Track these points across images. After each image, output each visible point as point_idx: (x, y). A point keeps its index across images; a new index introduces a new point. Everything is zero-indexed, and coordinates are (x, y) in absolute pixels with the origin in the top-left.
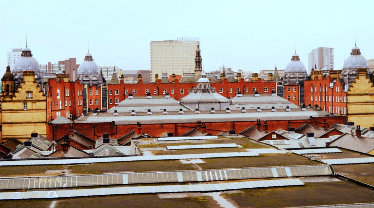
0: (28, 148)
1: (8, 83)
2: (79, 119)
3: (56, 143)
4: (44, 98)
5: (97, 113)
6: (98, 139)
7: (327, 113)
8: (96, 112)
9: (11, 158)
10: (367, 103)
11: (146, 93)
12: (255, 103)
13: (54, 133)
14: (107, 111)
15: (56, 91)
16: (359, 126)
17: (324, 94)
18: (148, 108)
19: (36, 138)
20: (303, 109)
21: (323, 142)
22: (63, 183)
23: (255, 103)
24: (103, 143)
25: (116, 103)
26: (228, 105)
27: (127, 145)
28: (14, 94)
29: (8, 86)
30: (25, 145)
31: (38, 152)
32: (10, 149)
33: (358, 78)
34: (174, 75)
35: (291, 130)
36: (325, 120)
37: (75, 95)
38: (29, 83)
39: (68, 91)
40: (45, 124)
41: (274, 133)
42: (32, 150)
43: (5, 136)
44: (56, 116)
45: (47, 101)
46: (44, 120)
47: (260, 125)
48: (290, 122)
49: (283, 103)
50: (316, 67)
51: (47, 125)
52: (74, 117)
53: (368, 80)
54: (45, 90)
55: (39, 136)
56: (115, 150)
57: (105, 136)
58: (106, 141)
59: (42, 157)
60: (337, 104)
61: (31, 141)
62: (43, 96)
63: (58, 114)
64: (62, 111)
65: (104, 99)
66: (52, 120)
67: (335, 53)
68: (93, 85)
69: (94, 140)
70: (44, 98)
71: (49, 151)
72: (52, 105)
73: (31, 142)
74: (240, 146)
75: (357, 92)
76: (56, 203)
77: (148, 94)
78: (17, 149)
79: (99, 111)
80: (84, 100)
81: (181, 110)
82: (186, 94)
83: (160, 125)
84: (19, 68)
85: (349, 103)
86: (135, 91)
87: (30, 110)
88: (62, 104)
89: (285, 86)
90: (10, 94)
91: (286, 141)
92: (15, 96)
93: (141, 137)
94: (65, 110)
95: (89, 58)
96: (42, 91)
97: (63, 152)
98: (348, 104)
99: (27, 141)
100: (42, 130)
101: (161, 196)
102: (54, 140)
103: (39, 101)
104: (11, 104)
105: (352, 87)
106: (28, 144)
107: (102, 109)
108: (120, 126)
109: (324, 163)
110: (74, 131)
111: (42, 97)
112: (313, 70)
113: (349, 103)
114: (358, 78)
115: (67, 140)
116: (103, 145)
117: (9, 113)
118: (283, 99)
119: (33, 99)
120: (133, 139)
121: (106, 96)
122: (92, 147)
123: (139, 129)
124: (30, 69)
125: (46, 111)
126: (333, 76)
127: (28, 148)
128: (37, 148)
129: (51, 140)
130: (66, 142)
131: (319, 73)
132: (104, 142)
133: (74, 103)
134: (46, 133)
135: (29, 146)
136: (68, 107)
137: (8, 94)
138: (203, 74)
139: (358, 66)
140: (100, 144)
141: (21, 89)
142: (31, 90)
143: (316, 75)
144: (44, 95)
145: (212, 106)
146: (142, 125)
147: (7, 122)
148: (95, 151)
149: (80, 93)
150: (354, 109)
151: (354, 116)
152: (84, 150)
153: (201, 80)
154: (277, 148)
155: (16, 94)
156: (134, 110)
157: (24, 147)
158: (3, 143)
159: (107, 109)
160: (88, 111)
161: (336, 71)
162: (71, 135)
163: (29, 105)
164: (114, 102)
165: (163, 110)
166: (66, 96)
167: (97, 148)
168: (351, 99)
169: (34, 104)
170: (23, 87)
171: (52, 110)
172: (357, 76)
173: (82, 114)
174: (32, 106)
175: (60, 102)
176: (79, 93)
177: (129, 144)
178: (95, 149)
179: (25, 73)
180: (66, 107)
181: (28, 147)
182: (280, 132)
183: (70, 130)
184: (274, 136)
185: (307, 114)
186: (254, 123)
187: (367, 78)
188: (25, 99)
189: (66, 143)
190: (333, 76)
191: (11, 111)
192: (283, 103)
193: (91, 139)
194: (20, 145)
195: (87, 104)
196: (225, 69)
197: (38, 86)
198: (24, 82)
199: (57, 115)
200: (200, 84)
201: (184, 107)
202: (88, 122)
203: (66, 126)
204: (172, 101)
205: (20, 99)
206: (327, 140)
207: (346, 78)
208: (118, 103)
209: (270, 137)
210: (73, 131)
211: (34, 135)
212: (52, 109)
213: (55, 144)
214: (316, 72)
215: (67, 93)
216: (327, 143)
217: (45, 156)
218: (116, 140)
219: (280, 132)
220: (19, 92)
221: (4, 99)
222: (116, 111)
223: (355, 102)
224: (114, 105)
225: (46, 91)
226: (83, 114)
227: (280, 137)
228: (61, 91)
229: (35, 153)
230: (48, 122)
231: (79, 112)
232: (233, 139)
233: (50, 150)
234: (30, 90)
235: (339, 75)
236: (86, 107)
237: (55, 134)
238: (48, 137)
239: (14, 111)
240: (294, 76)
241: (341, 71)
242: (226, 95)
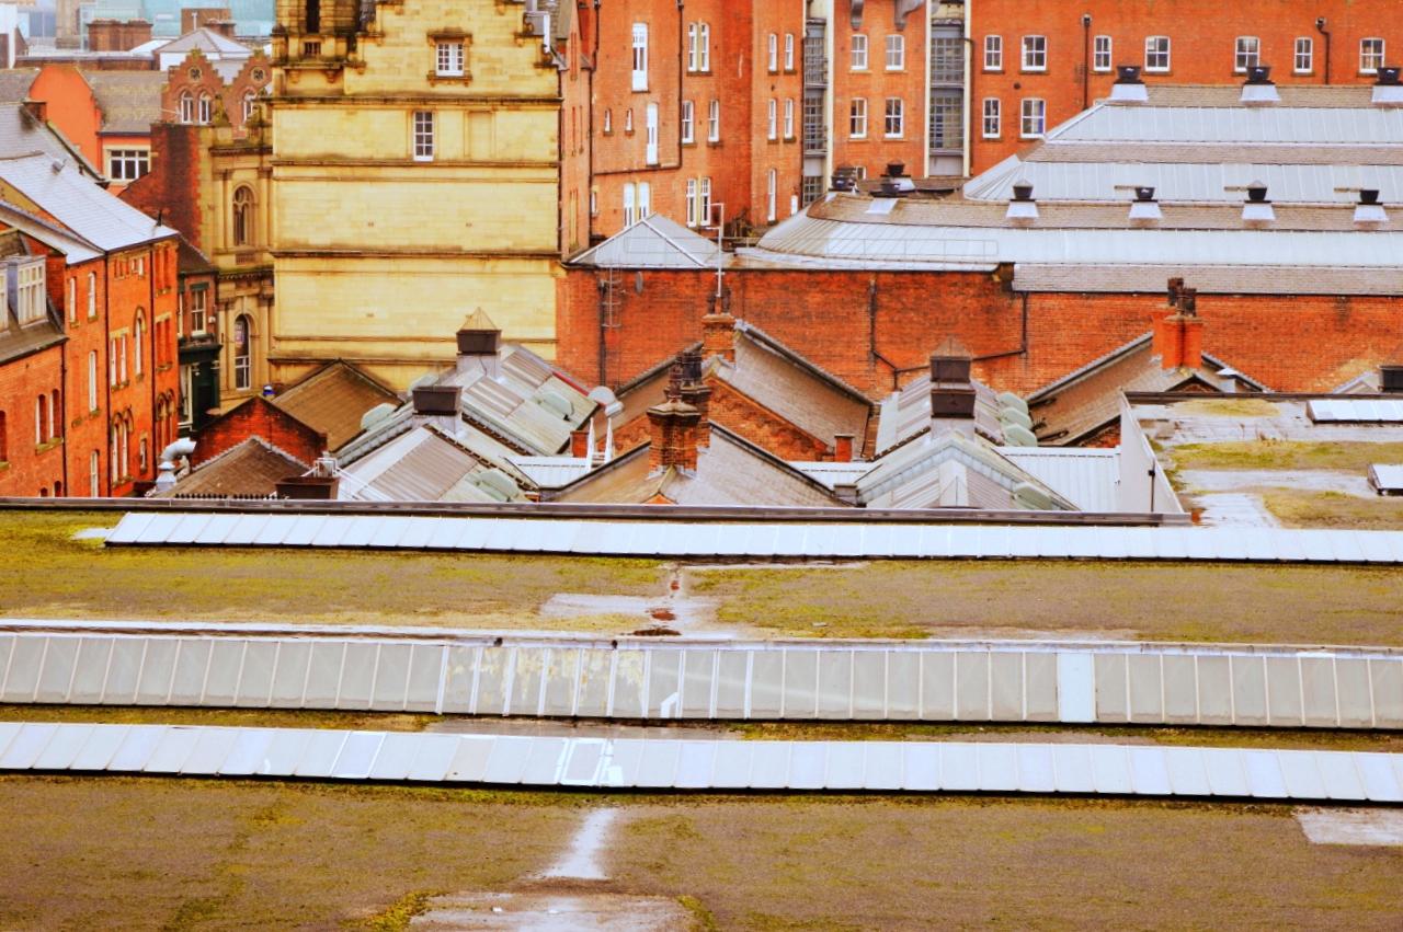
0: (434, 431)
2: (771, 237)
3: (618, 405)
4: (545, 83)
5: (893, 202)
6: (896, 388)
8: (889, 192)
9: (328, 497)
11: (1241, 60)
13: (603, 330)
14: (960, 189)
15: (625, 36)
18: (1251, 176)
19: (487, 360)
22: (661, 689)
24: (928, 421)
25: (1027, 130)
27: (1090, 438)
28: (352, 48)
30: (416, 406)
31: (500, 462)
32: (320, 430)
37: (749, 62)
39: (706, 33)
40: (546, 265)
42: (459, 446)
43: (289, 339)
44: (619, 214)
45: (565, 105)
51: (562, 273)
54: (554, 29)
55: (505, 351)
56: (1014, 472)
57: (941, 370)
58: (954, 406)
59: (522, 499)
61: (456, 381)
62: (537, 65)
63: (637, 195)
64: (658, 176)
65: (947, 98)
66: (595, 240)
69: (866, 396)
70: (545, 83)
71: (568, 458)
72: (598, 132)
73: (452, 394)
76: (615, 827)
77: (1252, 69)
78: (365, 431)
79: (905, 184)
80: (811, 106)
83: (1328, 307)
86: (1163, 46)
87: (453, 164)
88: (662, 124)
90: (330, 47)
92: (359, 66)
93: (1191, 389)
94: (680, 174)
96: (528, 33)
97: (661, 468)
99: (427, 384)
101: (1321, 828)
102: (602, 382)
103: (514, 102)
104: (332, 116)
106: (436, 402)
107: (926, 175)
108: (1050, 303)
110: (740, 325)
111: (531, 72)
115: (693, 386)
116: (927, 430)
117: (323, 184)
119: (477, 88)
120: (1136, 398)
121: (960, 77)
122: (856, 446)
123: (1183, 329)
125: (554, 173)
127: (434, 431)
128: (496, 436)
129: (584, 378)
130: (686, 398)
132: (937, 415)
133: (742, 121)
134: (551, 333)
135: (444, 419)
136: (702, 150)
137: (311, 50)
140: (904, 427)
141: (400, 13)
142: (465, 26)
144: (545, 64)
146: (1199, 303)
147: (308, 246)
148: (874, 477)
149: (781, 55)
152: (799, 465)
155: (366, 50)
156: (1152, 190)
157: (408, 424)
158: (278, 389)
159: (966, 174)
160: (837, 188)
162: (719, 352)
164: (1012, 123)
165: (1357, 197)
166: (693, 69)
167: (886, 453)
169: (481, 126)
171: (598, 168)
173: (795, 200)
174: (469, 137)
175: (652, 113)
177: (1105, 434)
178: (878, 457)
180: (684, 151)
181: (433, 421)
183: (710, 317)
188: (423, 86)
189: (682, 406)
193: (848, 386)
194: (386, 407)
195: (830, 135)
199: (629, 204)
202: (833, 265)
203: (686, 289)
205: (389, 83)
208: (1040, 131)
210: (727, 326)
211: (478, 343)
213: (608, 410)
215: (700, 57)
217: (542, 489)
218: (1017, 405)
220: (383, 35)
221: (291, 87)
222: (1023, 194)
224: (1019, 146)
225: (561, 36)
226: (801, 207)
228: (657, 34)
229: (480, 467)
230: (565, 255)
231: (772, 193)
233: (580, 452)
234: (453, 23)
236: (823, 158)
237: (608, 337)
238: (568, 362)
239: (347, 172)
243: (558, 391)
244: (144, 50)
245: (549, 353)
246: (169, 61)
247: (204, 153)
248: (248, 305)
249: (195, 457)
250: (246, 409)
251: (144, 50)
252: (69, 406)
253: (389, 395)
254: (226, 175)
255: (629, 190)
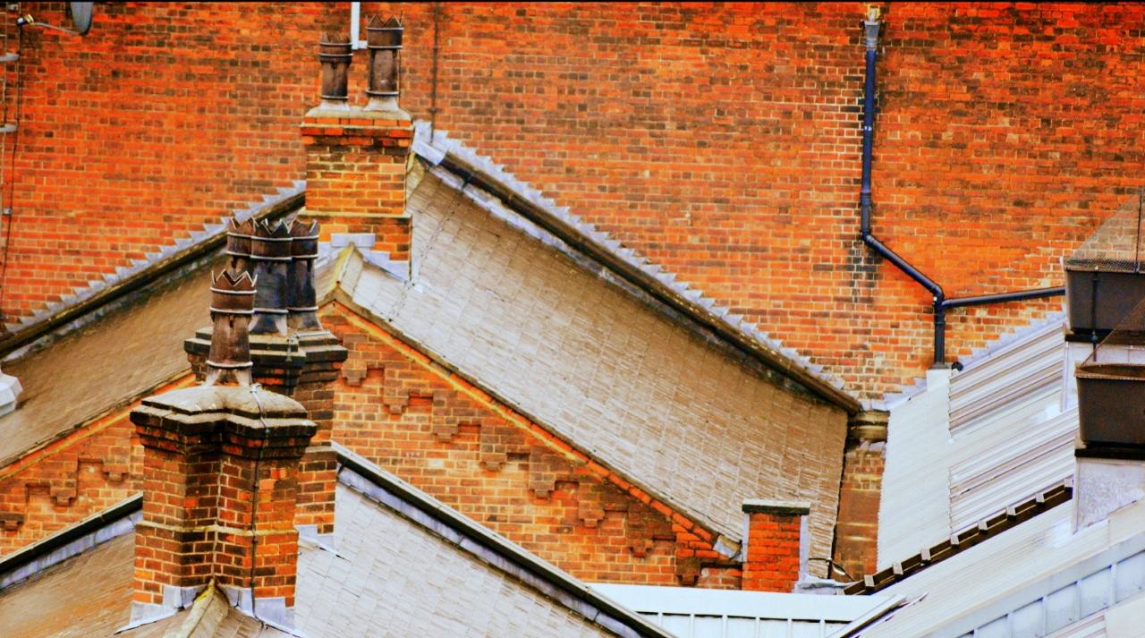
6: (939, 357)
69: (837, 380)
97: (174, 594)
110: (432, 143)
115: (285, 332)
122: (813, 538)
140: (971, 487)
162: (357, 227)
167: (914, 566)
178: (887, 579)
183: (329, 112)
193: (775, 346)
210: (388, 144)
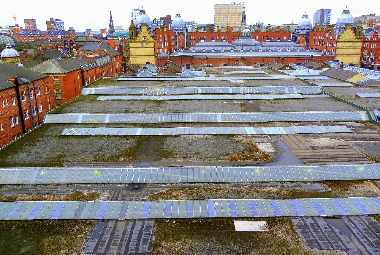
1: (133, 31)
4: (153, 40)
7: (322, 53)
10: (349, 47)
12: (277, 46)
16: (343, 62)
17: (322, 41)
18: (212, 48)
20: (307, 51)
21: (317, 72)
22: (165, 92)
23: (277, 46)
26: (260, 47)
27: (200, 70)
28: (136, 38)
29: (132, 32)
33: (345, 30)
34: (228, 27)
35: (299, 64)
36: (320, 58)
37: (170, 39)
38: (144, 32)
41: (288, 66)
46: (153, 53)
47: (279, 59)
48: (299, 59)
49: (294, 46)
50: (318, 23)
52: (170, 52)
53: (352, 31)
55: (150, 64)
57: (187, 65)
58: (188, 68)
60: (329, 47)
61: (146, 67)
63: (161, 50)
65: (187, 42)
67: (332, 13)
68: (181, 33)
73: (146, 67)
74: (266, 73)
75: (343, 40)
79: (184, 49)
80: (176, 42)
81: (232, 50)
82: (235, 39)
84: (139, 22)
85: (337, 47)
87: (145, 48)
89: (297, 35)
90: (134, 38)
91: (294, 71)
93: (208, 66)
95: (178, 15)
98: (337, 48)
100: (152, 60)
103: (150, 42)
104: (135, 44)
105: (341, 36)
106: (145, 68)
109: (317, 86)
112: (316, 24)
113: (337, 47)
114: (345, 30)
118: (295, 44)
119: (147, 41)
120: (203, 67)
123: (207, 61)
124: (145, 22)
126: (329, 28)
131: (320, 26)
133: (170, 44)
137: (132, 38)
138: (247, 26)
139: (347, 22)
143: (318, 28)
144: (153, 39)
145: (251, 47)
150: (340, 51)
151: (340, 56)
153: (245, 30)
154: (289, 75)
155: (137, 38)
161: (331, 25)
163: (145, 45)
164: (193, 44)
168: (339, 44)
169: (147, 44)
170: (141, 34)
172: (345, 29)
176: (173, 38)
177: (201, 70)
179: (142, 25)
182: (291, 65)
184: (288, 68)
185: (309, 53)
186: (276, 59)
187: (351, 30)
190: (329, 28)
191: (135, 48)
192: (294, 46)
196: (260, 24)
197: (149, 33)
198: (141, 30)
199: (160, 51)
200: (244, 33)
201: (234, 48)
203: (166, 58)
204: (227, 43)
205: (140, 41)
206: (321, 71)
207: (337, 30)
209: (285, 68)
211: (148, 63)
212: (157, 47)
214: (318, 26)
216: (320, 73)
218: (193, 68)
219: (291, 65)
223: (341, 46)
224: (193, 46)
227: (291, 68)
232: (262, 68)
235: (333, 28)
240: (304, 29)
241: (335, 25)
242: (260, 40)
243: (155, 67)
244: (118, 38)
245: (154, 64)
246: (120, 39)
247: (124, 47)
248: (128, 60)
249: (124, 73)
250: (128, 69)
251: (118, 38)
252: (113, 69)
253: (140, 68)
254: (126, 49)
255: (160, 50)
